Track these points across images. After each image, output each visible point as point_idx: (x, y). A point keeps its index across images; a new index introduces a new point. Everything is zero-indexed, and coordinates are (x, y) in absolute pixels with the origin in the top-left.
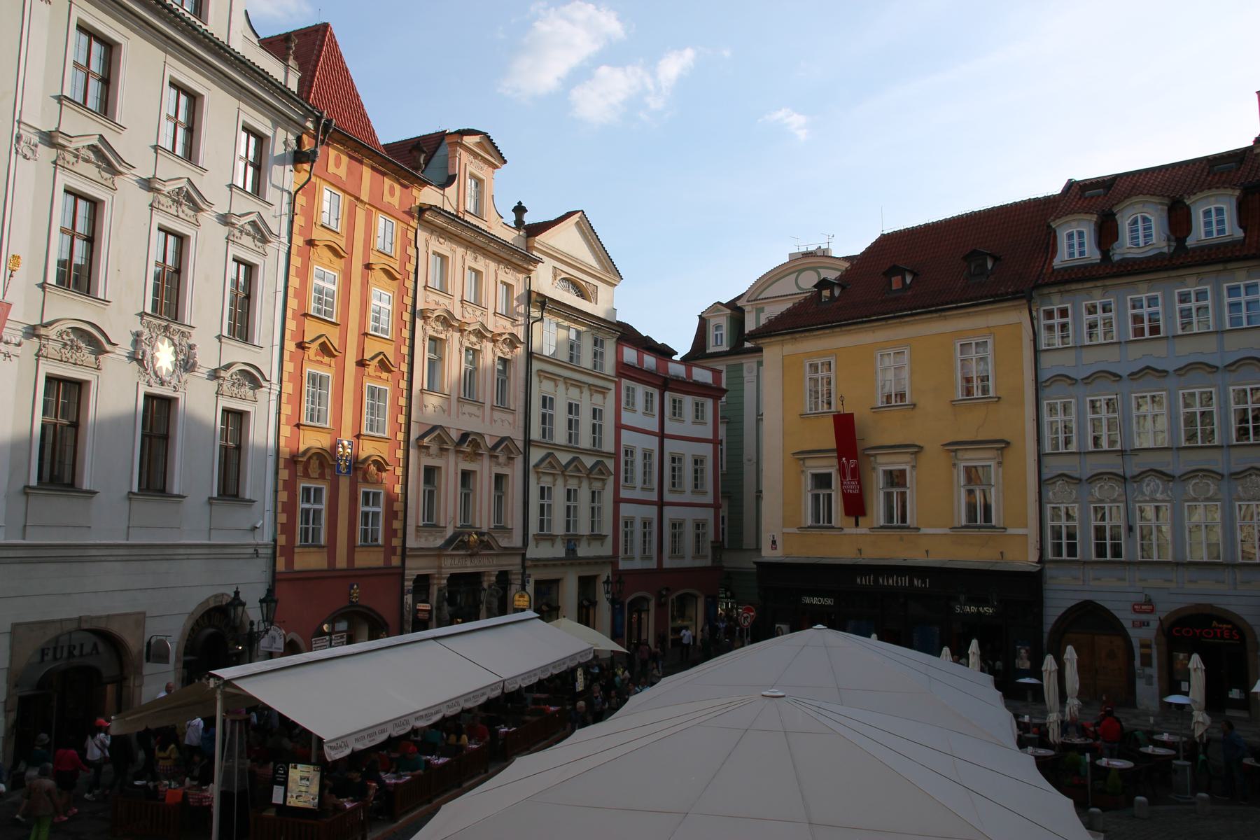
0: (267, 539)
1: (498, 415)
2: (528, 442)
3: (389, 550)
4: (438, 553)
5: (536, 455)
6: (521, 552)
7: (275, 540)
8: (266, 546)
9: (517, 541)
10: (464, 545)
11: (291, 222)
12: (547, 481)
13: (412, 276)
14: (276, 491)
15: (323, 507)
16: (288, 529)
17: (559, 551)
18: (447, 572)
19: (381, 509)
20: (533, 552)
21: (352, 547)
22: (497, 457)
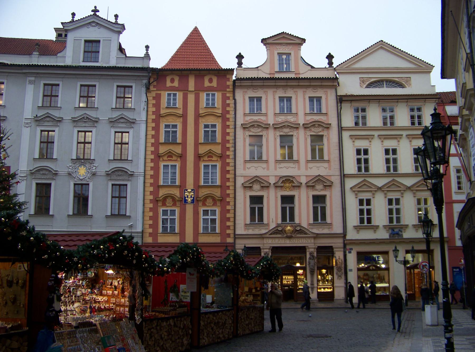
0: (139, 229)
1: (310, 165)
2: (343, 176)
3: (223, 234)
4: (261, 237)
5: (350, 183)
6: (344, 235)
7: (143, 231)
8: (137, 232)
9: (338, 229)
10: (283, 232)
11: (147, 111)
12: (365, 196)
13: (232, 113)
14: (143, 212)
15: (177, 217)
16: (154, 226)
17: (383, 234)
18: (268, 246)
19: (217, 217)
20: (352, 235)
21: (196, 233)
22: (313, 186)
